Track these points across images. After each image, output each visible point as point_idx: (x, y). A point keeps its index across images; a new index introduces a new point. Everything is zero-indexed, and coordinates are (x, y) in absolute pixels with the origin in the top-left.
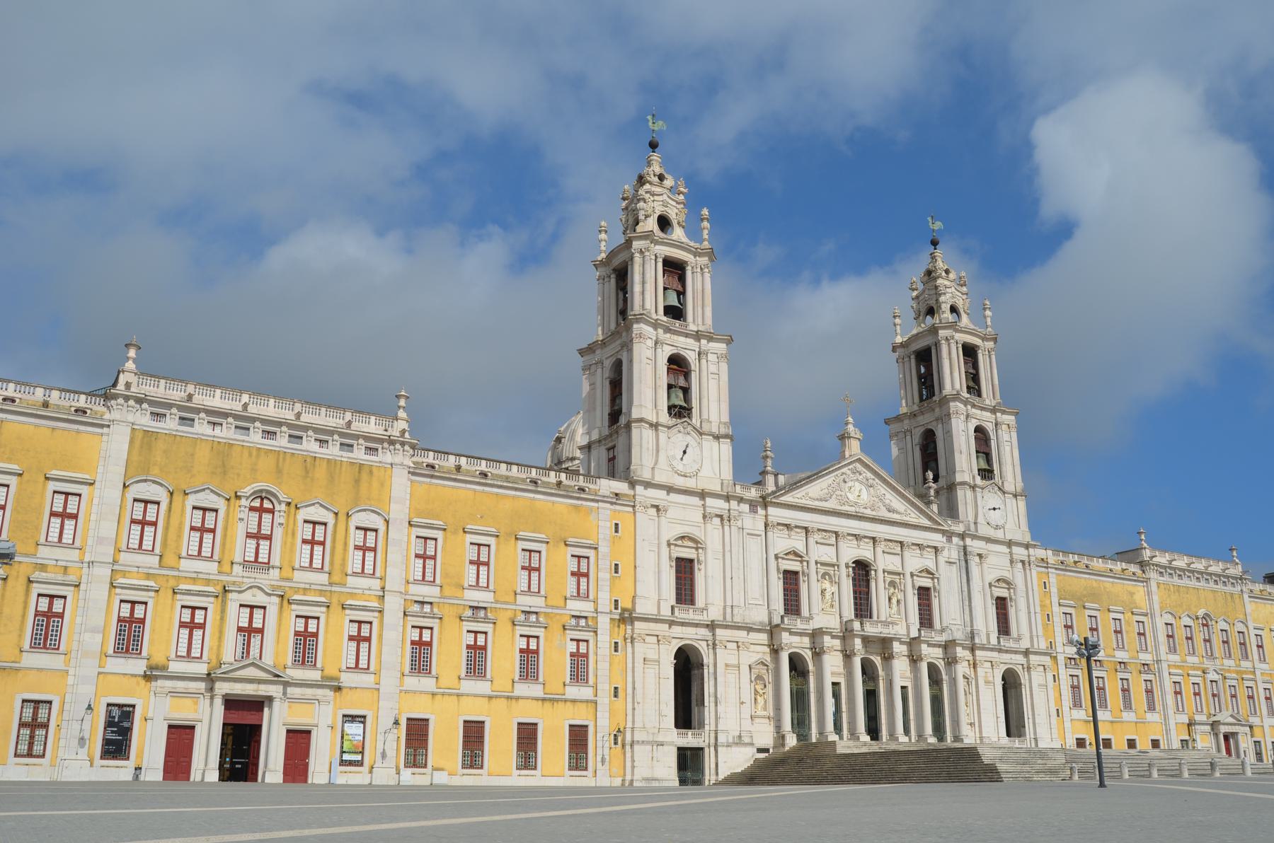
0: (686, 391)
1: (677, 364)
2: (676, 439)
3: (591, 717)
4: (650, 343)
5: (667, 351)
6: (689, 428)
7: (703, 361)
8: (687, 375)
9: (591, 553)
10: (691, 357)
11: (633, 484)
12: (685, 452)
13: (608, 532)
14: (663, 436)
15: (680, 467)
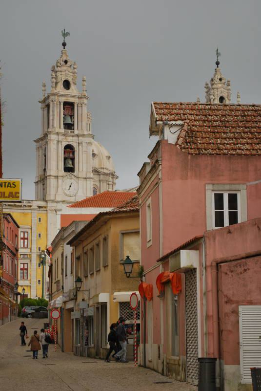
0: (73, 159)
1: (69, 148)
2: (68, 180)
3: (29, 292)
4: (55, 142)
5: (64, 144)
6: (73, 177)
7: (80, 147)
8: (73, 153)
9: (29, 231)
10: (75, 145)
11: (46, 201)
12: (70, 186)
13: (36, 221)
14: (60, 181)
15: (68, 192)
